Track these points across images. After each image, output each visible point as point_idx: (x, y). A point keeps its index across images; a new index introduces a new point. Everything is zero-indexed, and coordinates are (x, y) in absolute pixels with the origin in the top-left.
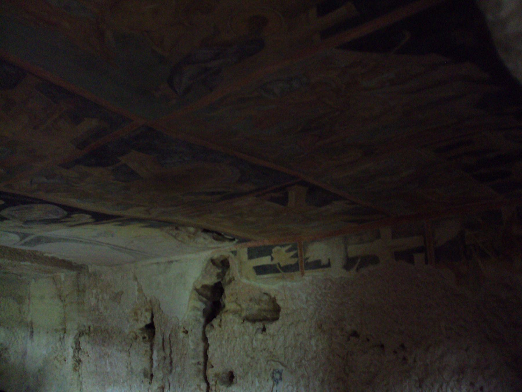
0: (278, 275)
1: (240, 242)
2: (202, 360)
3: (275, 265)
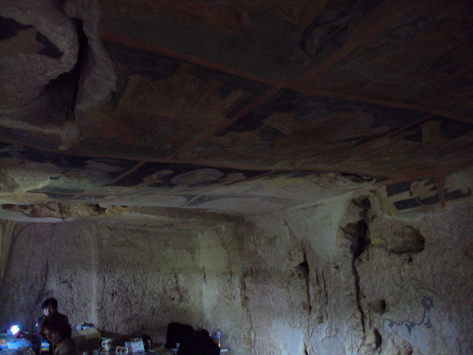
0: (420, 207)
1: (377, 181)
2: (354, 291)
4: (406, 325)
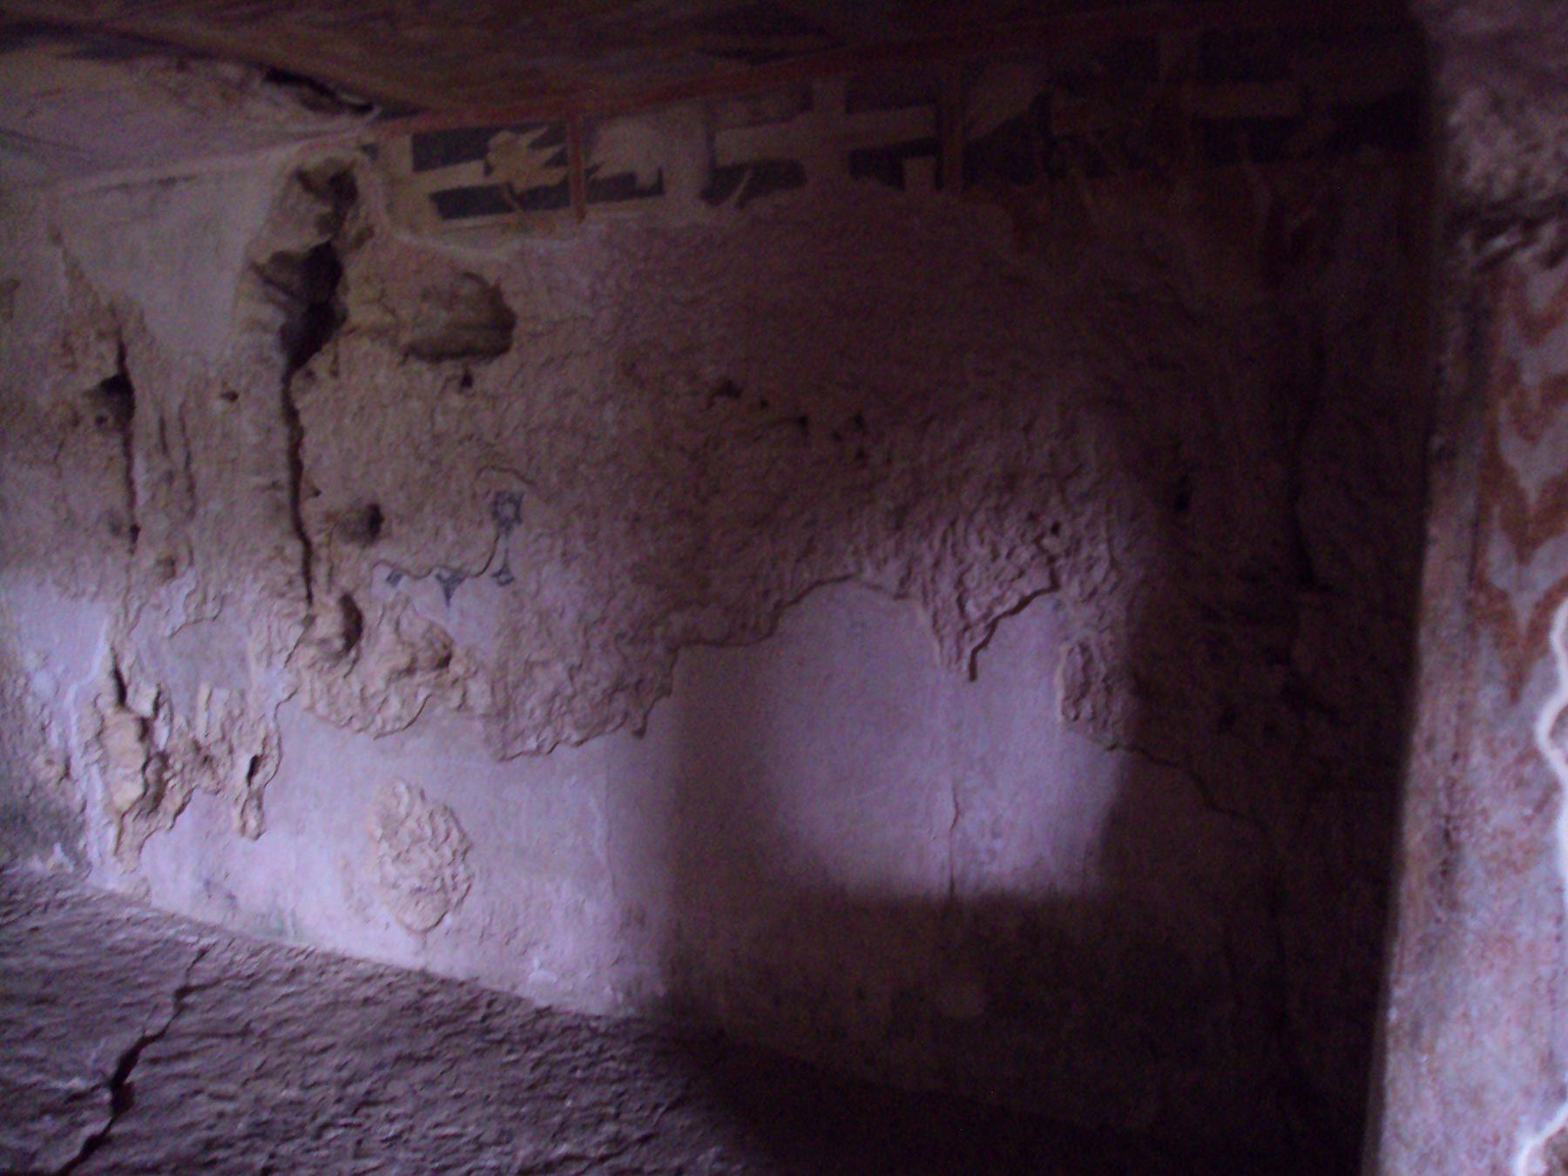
0: (507, 218)
1: (385, 116)
2: (284, 476)
3: (496, 188)
4: (439, 577)
